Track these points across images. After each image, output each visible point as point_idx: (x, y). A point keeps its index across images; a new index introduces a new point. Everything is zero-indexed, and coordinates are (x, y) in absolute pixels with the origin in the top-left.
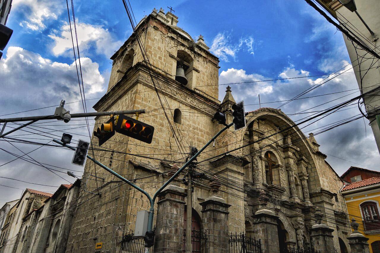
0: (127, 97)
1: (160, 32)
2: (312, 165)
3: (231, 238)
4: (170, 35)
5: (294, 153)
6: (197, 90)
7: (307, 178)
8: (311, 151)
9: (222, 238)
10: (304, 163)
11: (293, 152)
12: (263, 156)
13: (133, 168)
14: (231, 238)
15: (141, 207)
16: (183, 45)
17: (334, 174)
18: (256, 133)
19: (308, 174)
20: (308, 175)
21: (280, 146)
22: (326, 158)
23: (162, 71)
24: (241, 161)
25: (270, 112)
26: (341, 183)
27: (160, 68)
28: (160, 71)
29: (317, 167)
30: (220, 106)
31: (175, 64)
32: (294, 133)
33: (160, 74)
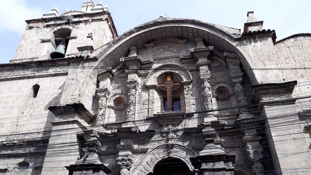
8: (232, 39)
10: (231, 61)
18: (130, 63)
24: (69, 108)
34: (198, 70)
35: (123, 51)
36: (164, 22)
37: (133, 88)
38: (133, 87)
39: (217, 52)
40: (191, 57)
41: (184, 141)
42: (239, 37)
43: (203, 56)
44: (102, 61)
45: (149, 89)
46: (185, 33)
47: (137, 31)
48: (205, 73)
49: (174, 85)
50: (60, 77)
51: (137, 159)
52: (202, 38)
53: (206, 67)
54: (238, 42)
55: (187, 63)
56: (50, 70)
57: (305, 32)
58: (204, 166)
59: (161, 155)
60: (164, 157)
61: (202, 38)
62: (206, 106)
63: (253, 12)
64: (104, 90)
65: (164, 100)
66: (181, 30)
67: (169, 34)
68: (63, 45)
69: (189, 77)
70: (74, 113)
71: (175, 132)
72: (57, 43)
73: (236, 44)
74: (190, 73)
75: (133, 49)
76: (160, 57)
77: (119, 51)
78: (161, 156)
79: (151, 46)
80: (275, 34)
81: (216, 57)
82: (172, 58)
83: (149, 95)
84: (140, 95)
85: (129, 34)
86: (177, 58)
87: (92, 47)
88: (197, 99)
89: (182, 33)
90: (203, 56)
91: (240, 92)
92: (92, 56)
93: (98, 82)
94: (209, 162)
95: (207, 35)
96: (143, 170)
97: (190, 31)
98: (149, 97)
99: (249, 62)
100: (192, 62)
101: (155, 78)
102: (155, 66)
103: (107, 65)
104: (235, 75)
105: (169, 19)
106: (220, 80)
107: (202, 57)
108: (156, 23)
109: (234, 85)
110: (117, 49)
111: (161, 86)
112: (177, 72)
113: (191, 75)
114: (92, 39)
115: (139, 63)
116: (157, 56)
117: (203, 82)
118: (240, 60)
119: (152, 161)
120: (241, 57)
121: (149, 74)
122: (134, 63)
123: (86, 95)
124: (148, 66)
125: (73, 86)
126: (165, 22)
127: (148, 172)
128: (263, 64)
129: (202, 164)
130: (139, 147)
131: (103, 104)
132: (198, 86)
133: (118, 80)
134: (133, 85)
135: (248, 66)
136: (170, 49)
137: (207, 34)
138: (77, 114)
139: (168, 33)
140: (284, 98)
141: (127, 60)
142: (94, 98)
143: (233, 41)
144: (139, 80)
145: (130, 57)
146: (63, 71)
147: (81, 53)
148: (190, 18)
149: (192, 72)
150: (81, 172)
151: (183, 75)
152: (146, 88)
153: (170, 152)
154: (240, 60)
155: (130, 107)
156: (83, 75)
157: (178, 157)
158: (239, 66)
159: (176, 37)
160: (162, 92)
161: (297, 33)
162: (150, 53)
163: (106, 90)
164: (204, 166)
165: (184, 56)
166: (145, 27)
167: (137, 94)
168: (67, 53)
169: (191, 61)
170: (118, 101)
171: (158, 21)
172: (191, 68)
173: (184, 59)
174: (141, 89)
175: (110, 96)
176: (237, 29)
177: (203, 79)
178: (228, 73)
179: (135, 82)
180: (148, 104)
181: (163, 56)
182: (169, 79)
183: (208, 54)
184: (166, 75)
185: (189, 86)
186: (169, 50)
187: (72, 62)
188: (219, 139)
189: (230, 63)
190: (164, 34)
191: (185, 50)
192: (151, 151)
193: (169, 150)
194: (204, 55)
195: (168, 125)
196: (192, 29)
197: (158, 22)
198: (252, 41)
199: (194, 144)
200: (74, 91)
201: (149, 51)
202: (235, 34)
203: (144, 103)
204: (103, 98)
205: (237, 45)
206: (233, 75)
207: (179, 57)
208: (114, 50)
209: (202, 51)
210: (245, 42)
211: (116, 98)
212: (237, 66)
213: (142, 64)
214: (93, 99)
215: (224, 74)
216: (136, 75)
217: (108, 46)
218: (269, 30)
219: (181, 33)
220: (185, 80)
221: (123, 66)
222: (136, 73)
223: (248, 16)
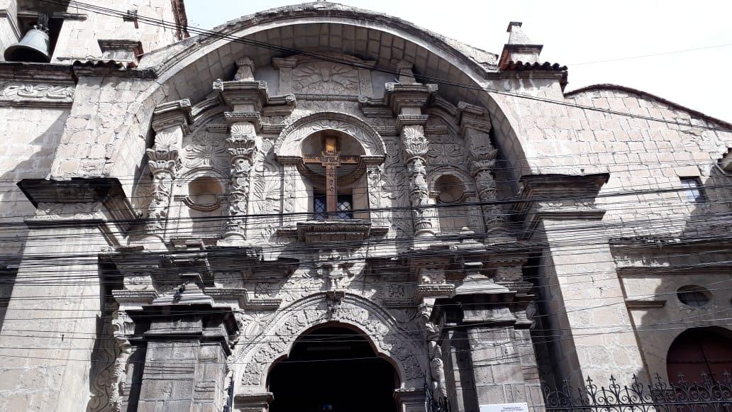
8: (479, 74)
10: (472, 121)
29: (514, 113)
32: (405, 47)
34: (399, 134)
35: (221, 65)
36: (327, 11)
37: (245, 159)
38: (246, 155)
39: (441, 99)
40: (385, 104)
41: (364, 288)
42: (496, 71)
43: (412, 104)
44: (168, 82)
45: (283, 166)
46: (374, 46)
47: (260, 23)
48: (417, 143)
49: (342, 162)
50: (36, 114)
51: (250, 326)
52: (410, 62)
53: (418, 130)
54: (491, 82)
55: (374, 116)
56: (7, 90)
57: (615, 83)
58: (469, 316)
59: (313, 316)
60: (318, 320)
61: (410, 62)
62: (418, 213)
63: (520, 24)
64: (169, 155)
65: (318, 196)
66: (365, 37)
67: (335, 42)
68: (42, 32)
69: (378, 148)
70: (93, 202)
71: (345, 267)
72: (25, 25)
73: (487, 85)
74: (381, 139)
75: (247, 65)
76: (311, 93)
77: (210, 64)
78: (310, 319)
79: (291, 65)
80: (565, 75)
81: (439, 111)
82: (340, 100)
83: (282, 180)
84: (260, 177)
85: (240, 25)
86: (351, 103)
87: (140, 43)
88: (395, 199)
89: (367, 45)
90: (412, 104)
91: (489, 189)
92: (142, 65)
93: (152, 134)
94: (481, 308)
95: (426, 57)
96: (267, 348)
97: (386, 42)
98: (282, 184)
99: (513, 127)
100: (385, 114)
101: (298, 140)
102: (298, 113)
103: (178, 93)
104: (480, 152)
105: (339, 6)
106: (446, 161)
107: (411, 107)
108: (308, 10)
109: (476, 175)
110: (207, 58)
111: (312, 161)
112: (350, 133)
113: (383, 143)
114: (137, 27)
115: (260, 102)
116: (304, 91)
117: (412, 161)
118: (491, 122)
119: (288, 329)
120: (495, 116)
121: (284, 130)
122: (249, 100)
123: (123, 162)
124: (282, 109)
125: (87, 134)
126: (329, 13)
127: (280, 355)
128: (542, 135)
129: (465, 312)
130: (256, 297)
131: (165, 190)
132: (398, 170)
133: (201, 136)
134: (245, 151)
135: (509, 136)
136: (335, 78)
137: (425, 55)
138: (101, 204)
139: (333, 40)
140: (583, 208)
141: (231, 87)
142: (139, 173)
143: (481, 77)
144: (259, 141)
145: (240, 83)
146: (48, 97)
147: (109, 56)
148: (390, 13)
149: (386, 138)
150: (172, 323)
151: (365, 142)
152: (276, 162)
153: (333, 311)
154: (491, 122)
155: (237, 202)
156: (115, 110)
157: (350, 322)
158: (488, 136)
159: (348, 53)
160: (313, 177)
161: (601, 83)
162: (287, 82)
163: (172, 156)
164: (469, 316)
165: (370, 99)
166: (282, 17)
167: (253, 174)
168: (56, 54)
169: (383, 111)
170: (200, 186)
171: (315, 6)
172: (381, 127)
173: (368, 105)
174: (262, 163)
175: (181, 172)
176: (491, 54)
177: (412, 156)
178: (462, 148)
179: (251, 143)
180: (282, 199)
181: (318, 92)
182: (330, 148)
183: (425, 101)
184: (324, 137)
185: (379, 167)
186: (332, 81)
187: (86, 75)
188: (444, 284)
189: (468, 126)
190: (324, 40)
191: (371, 85)
192: (289, 307)
193: (330, 306)
194: (415, 103)
195: (329, 250)
196: (393, 40)
197: (315, 10)
198: (521, 83)
199: (387, 295)
200: (90, 147)
201: (283, 75)
202: (486, 64)
203: (271, 197)
204: (164, 174)
205: (489, 88)
206: (476, 153)
207: (356, 101)
208: (201, 59)
209: (412, 92)
210: (506, 84)
211: (196, 177)
212: (485, 134)
213: (266, 105)
214: (136, 173)
215: (455, 150)
216: (253, 127)
217: (187, 48)
218: (556, 65)
219: (365, 44)
220: (368, 153)
221: (218, 102)
222: (252, 121)
223: (509, 30)
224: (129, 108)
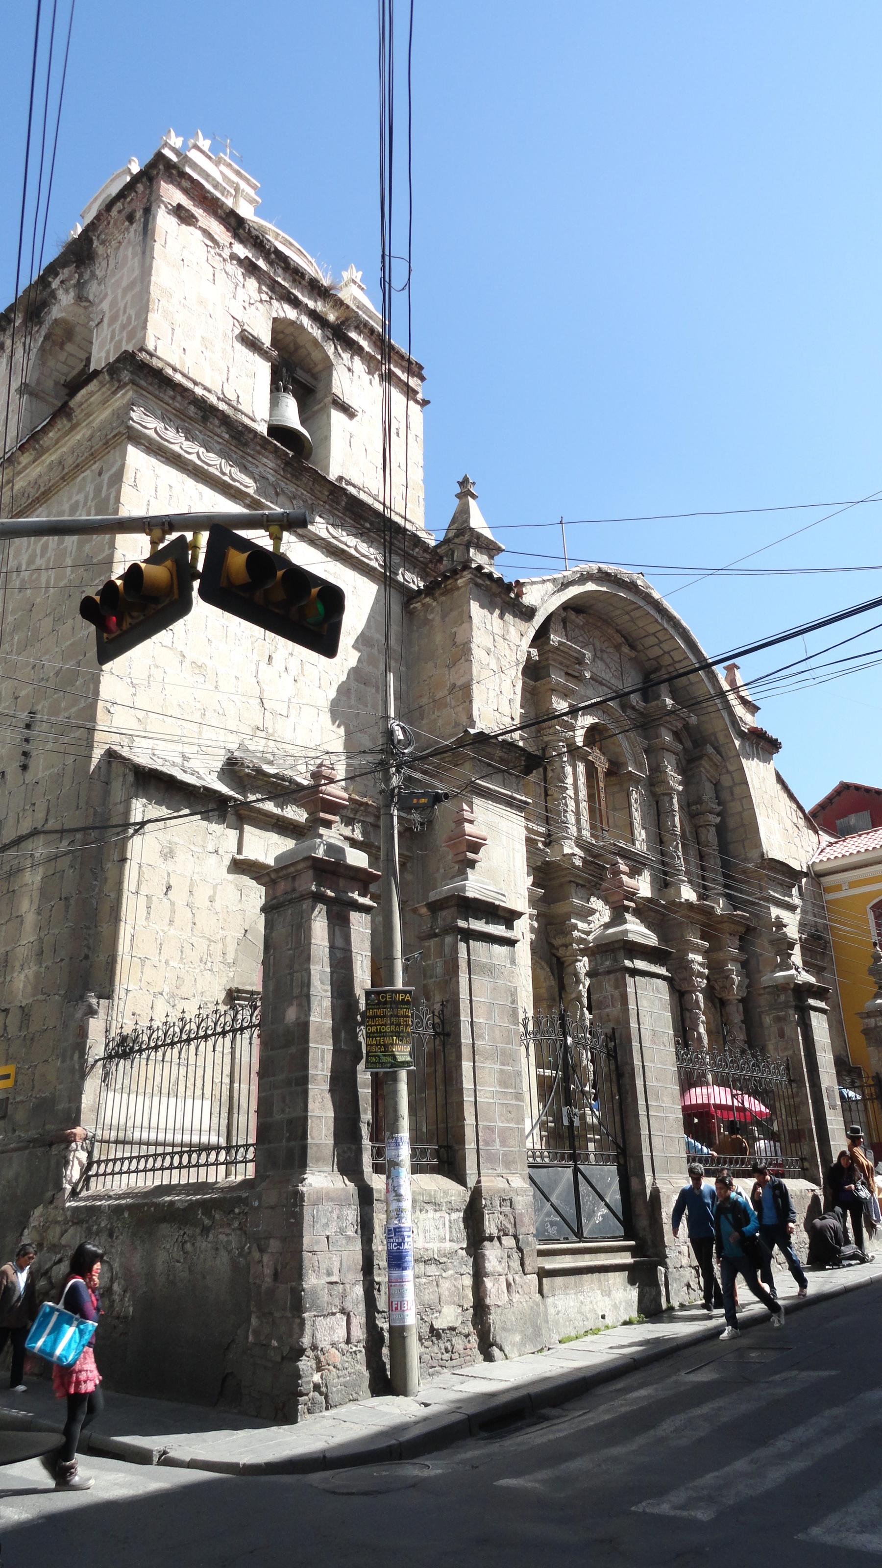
0: (81, 497)
1: (198, 233)
2: (735, 775)
3: (525, 1026)
4: (242, 251)
5: (676, 735)
6: (349, 483)
7: (718, 820)
9: (501, 1032)
11: (675, 729)
12: (579, 741)
13: (131, 778)
14: (525, 1026)
15: (166, 929)
16: (295, 303)
17: (794, 806)
19: (719, 804)
20: (720, 808)
21: (633, 708)
22: (778, 752)
23: (219, 398)
25: (609, 581)
26: (814, 837)
27: (208, 384)
28: (213, 399)
30: (436, 555)
31: (264, 369)
33: (213, 409)
136: (605, 656)
187: (477, 585)
219: (644, 634)
224: (519, 653)
